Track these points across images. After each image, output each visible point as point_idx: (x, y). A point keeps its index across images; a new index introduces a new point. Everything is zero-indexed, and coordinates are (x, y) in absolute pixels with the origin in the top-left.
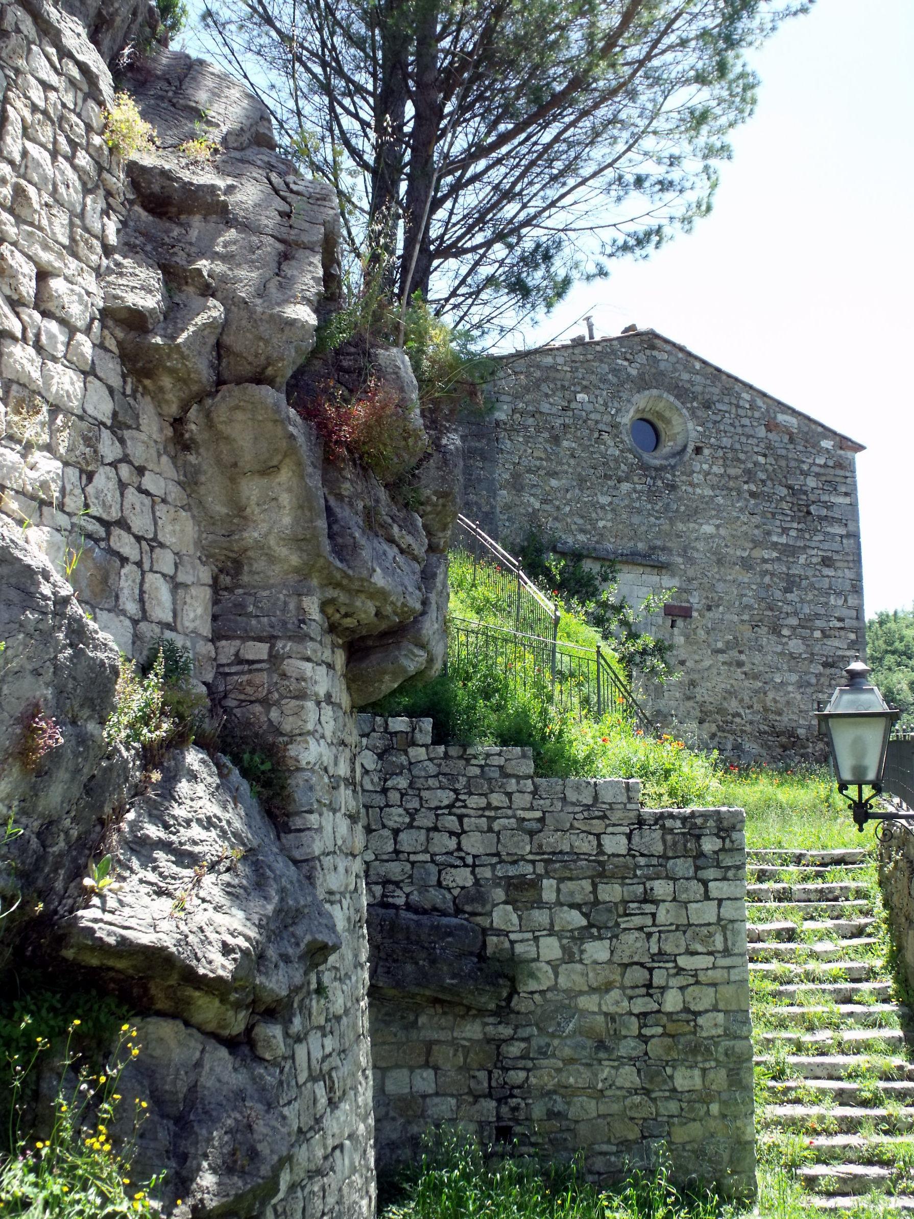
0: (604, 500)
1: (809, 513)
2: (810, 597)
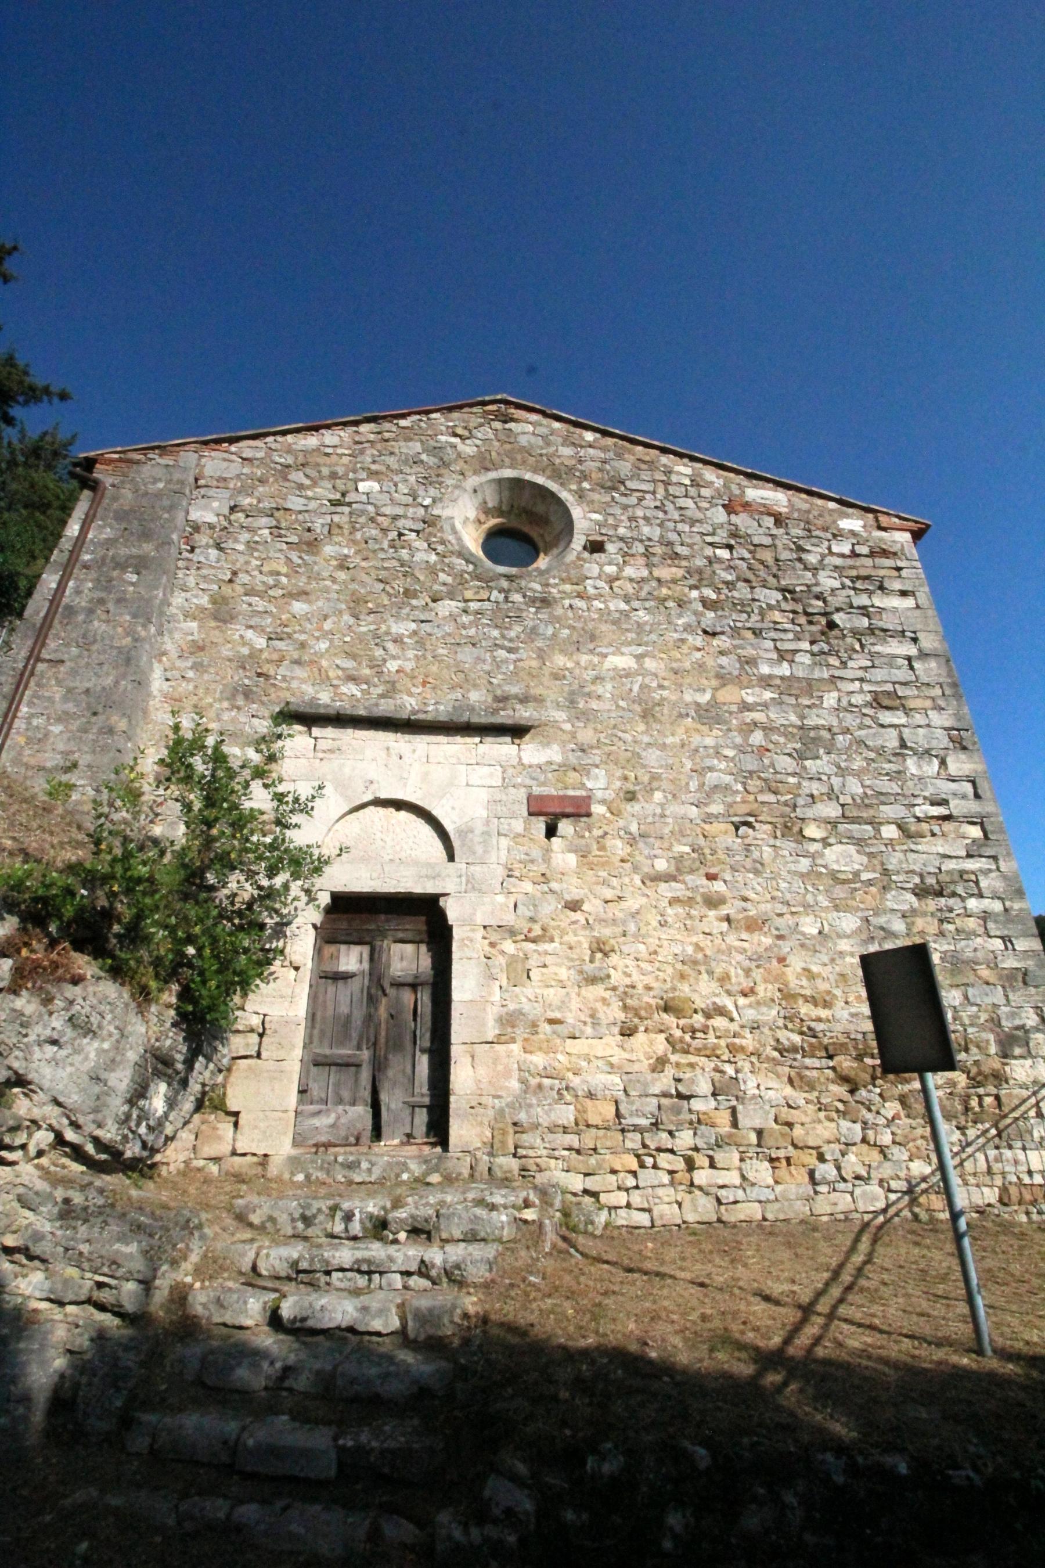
0: (403, 628)
1: (832, 625)
2: (858, 764)
